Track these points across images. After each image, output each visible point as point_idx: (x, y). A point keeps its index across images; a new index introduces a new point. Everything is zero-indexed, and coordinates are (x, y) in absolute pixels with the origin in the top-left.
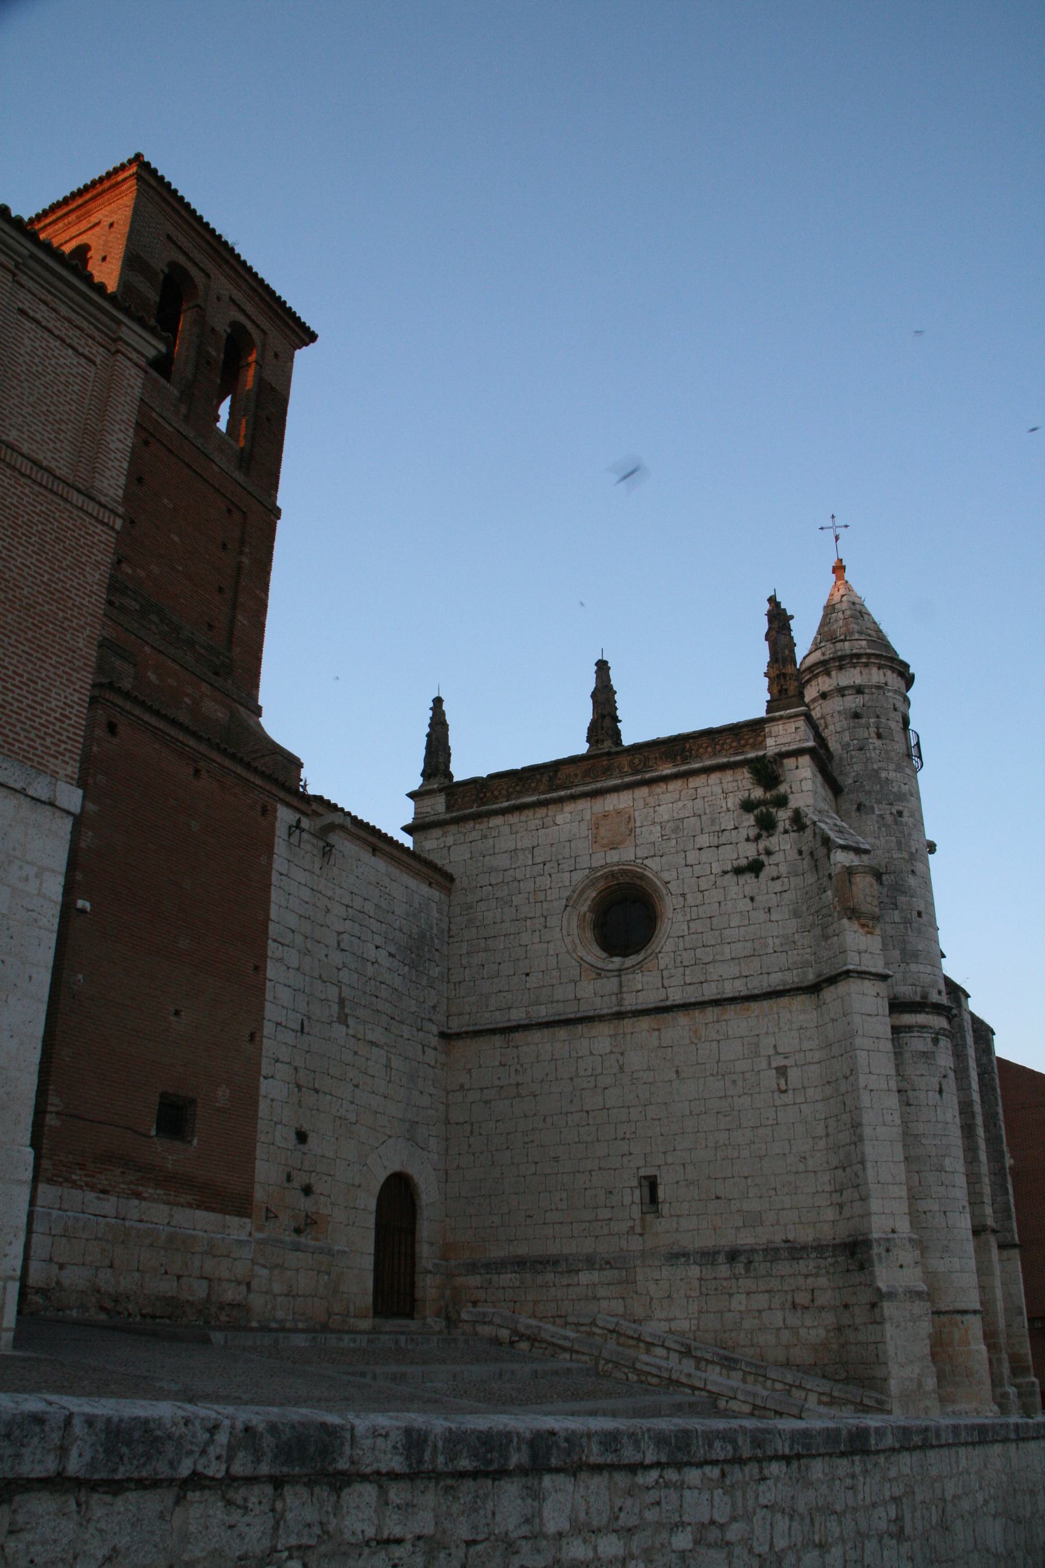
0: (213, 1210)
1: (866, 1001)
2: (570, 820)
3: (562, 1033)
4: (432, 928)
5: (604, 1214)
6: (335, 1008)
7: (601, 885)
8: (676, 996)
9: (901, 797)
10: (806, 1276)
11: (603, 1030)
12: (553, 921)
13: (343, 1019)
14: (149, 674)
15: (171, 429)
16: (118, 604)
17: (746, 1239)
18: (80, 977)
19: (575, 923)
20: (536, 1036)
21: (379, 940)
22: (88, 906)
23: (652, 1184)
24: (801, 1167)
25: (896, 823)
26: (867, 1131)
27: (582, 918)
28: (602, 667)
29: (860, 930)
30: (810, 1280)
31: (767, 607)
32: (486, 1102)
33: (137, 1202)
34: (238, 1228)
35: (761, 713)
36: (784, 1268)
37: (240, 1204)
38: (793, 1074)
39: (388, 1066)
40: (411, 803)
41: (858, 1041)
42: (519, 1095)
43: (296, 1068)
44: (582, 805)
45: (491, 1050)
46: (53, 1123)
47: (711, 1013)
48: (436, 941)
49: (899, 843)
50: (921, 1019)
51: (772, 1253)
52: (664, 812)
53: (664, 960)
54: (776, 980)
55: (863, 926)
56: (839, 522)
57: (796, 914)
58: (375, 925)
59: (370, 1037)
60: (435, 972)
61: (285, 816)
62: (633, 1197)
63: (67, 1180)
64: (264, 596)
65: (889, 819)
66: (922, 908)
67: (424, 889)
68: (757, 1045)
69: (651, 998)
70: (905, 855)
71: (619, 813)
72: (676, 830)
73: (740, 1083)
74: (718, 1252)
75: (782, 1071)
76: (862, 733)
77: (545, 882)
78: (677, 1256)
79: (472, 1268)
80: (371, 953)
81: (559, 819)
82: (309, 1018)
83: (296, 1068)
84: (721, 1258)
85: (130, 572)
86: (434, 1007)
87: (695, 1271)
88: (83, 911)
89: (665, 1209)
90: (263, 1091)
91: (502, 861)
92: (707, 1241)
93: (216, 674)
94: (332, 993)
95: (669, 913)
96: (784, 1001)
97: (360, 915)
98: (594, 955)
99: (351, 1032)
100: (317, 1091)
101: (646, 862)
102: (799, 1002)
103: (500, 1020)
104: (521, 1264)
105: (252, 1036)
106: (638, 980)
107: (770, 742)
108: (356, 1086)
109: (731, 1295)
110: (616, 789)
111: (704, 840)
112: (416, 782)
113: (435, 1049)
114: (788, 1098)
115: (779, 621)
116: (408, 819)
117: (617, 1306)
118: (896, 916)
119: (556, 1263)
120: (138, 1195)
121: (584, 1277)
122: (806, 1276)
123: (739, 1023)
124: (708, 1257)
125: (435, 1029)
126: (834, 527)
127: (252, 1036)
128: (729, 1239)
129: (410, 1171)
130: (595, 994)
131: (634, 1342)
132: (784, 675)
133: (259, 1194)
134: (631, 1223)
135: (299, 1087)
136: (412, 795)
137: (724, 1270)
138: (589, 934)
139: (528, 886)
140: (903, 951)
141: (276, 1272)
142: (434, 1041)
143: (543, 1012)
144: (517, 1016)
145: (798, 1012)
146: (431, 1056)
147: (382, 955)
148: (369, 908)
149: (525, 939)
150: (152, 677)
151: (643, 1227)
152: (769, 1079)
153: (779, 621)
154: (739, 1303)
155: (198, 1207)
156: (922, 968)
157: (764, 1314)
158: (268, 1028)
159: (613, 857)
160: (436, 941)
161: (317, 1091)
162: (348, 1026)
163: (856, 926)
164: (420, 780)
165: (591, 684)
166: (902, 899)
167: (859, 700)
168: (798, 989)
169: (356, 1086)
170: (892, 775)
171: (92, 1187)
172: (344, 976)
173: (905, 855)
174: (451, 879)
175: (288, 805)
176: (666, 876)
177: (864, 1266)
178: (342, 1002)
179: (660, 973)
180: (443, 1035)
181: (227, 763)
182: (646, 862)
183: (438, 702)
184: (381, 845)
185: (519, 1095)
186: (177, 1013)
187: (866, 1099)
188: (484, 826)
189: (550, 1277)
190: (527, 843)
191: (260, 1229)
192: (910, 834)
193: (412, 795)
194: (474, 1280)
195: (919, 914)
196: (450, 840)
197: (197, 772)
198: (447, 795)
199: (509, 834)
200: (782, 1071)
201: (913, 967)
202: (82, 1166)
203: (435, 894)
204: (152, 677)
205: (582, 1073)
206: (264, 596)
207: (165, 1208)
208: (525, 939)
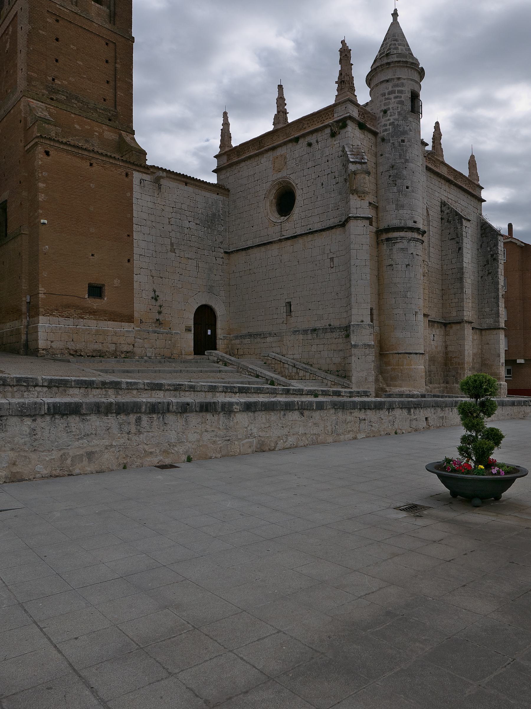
0: (116, 321)
3: (263, 249)
4: (219, 211)
5: (275, 316)
6: (169, 247)
7: (277, 187)
9: (404, 133)
10: (335, 338)
11: (275, 246)
13: (173, 251)
14: (75, 126)
15: (68, 11)
16: (55, 99)
17: (318, 325)
18: (47, 247)
19: (268, 204)
20: (256, 250)
21: (190, 219)
22: (46, 221)
23: (289, 304)
24: (337, 297)
25: (400, 145)
26: (353, 282)
29: (358, 199)
30: (337, 340)
31: (341, 46)
32: (241, 277)
33: (82, 320)
34: (127, 327)
36: (328, 335)
37: (130, 319)
39: (197, 266)
41: (352, 246)
42: (250, 274)
43: (151, 270)
44: (270, 154)
45: (241, 257)
46: (43, 297)
47: (310, 237)
48: (221, 216)
49: (400, 156)
50: (402, 234)
51: (325, 330)
55: (359, 197)
57: (340, 194)
58: (188, 213)
59: (187, 256)
61: (137, 176)
62: (283, 310)
63: (51, 315)
64: (130, 81)
65: (397, 144)
66: (409, 184)
67: (215, 196)
68: (324, 249)
70: (403, 161)
72: (300, 161)
73: (318, 265)
74: (308, 330)
78: (296, 331)
79: (237, 337)
80: (186, 224)
82: (156, 251)
83: (151, 270)
84: (309, 332)
85: (60, 83)
86: (221, 242)
87: (301, 337)
88: (44, 224)
89: (293, 314)
90: (135, 279)
92: (305, 326)
93: (110, 120)
94: (167, 241)
96: (334, 230)
97: (180, 210)
99: (177, 255)
100: (162, 278)
101: (291, 176)
102: (339, 231)
104: (250, 335)
105: (129, 261)
106: (287, 226)
107: (335, 115)
108: (182, 275)
109: (312, 345)
110: (280, 146)
111: (310, 164)
112: (217, 151)
113: (222, 258)
114: (333, 270)
116: (215, 167)
117: (278, 350)
118: (395, 189)
119: (260, 335)
120: (82, 318)
121: (269, 339)
122: (335, 338)
123: (320, 240)
124: (305, 332)
125: (222, 251)
127: (129, 261)
128: (312, 325)
129: (210, 303)
131: (279, 362)
132: (344, 81)
133: (136, 315)
134: (283, 320)
135: (152, 276)
137: (310, 336)
138: (274, 208)
140: (397, 205)
141: (146, 340)
142: (222, 255)
143: (257, 242)
144: (250, 244)
146: (220, 261)
147: (192, 225)
148: (184, 206)
150: (77, 127)
151: (287, 321)
153: (345, 54)
154: (314, 348)
155: (109, 320)
156: (405, 212)
157: (322, 352)
158: (136, 257)
159: (280, 175)
160: (221, 216)
161: (162, 278)
162: (175, 253)
163: (356, 197)
165: (276, 96)
168: (338, 225)
169: (182, 275)
170: (401, 122)
171: (62, 316)
172: (173, 234)
173: (403, 161)
174: (228, 190)
175: (138, 171)
177: (348, 336)
178: (172, 244)
180: (226, 252)
181: (104, 159)
182: (291, 176)
184: (188, 181)
185: (250, 274)
186: (93, 255)
188: (238, 167)
189: (259, 340)
191: (137, 327)
192: (407, 150)
194: (238, 341)
195: (407, 188)
196: (228, 174)
197: (91, 165)
198: (227, 155)
199: (246, 170)
200: (332, 259)
201: (401, 212)
202: (57, 310)
203: (220, 197)
204: (77, 127)
205: (269, 263)
206: (130, 81)
207: (95, 321)
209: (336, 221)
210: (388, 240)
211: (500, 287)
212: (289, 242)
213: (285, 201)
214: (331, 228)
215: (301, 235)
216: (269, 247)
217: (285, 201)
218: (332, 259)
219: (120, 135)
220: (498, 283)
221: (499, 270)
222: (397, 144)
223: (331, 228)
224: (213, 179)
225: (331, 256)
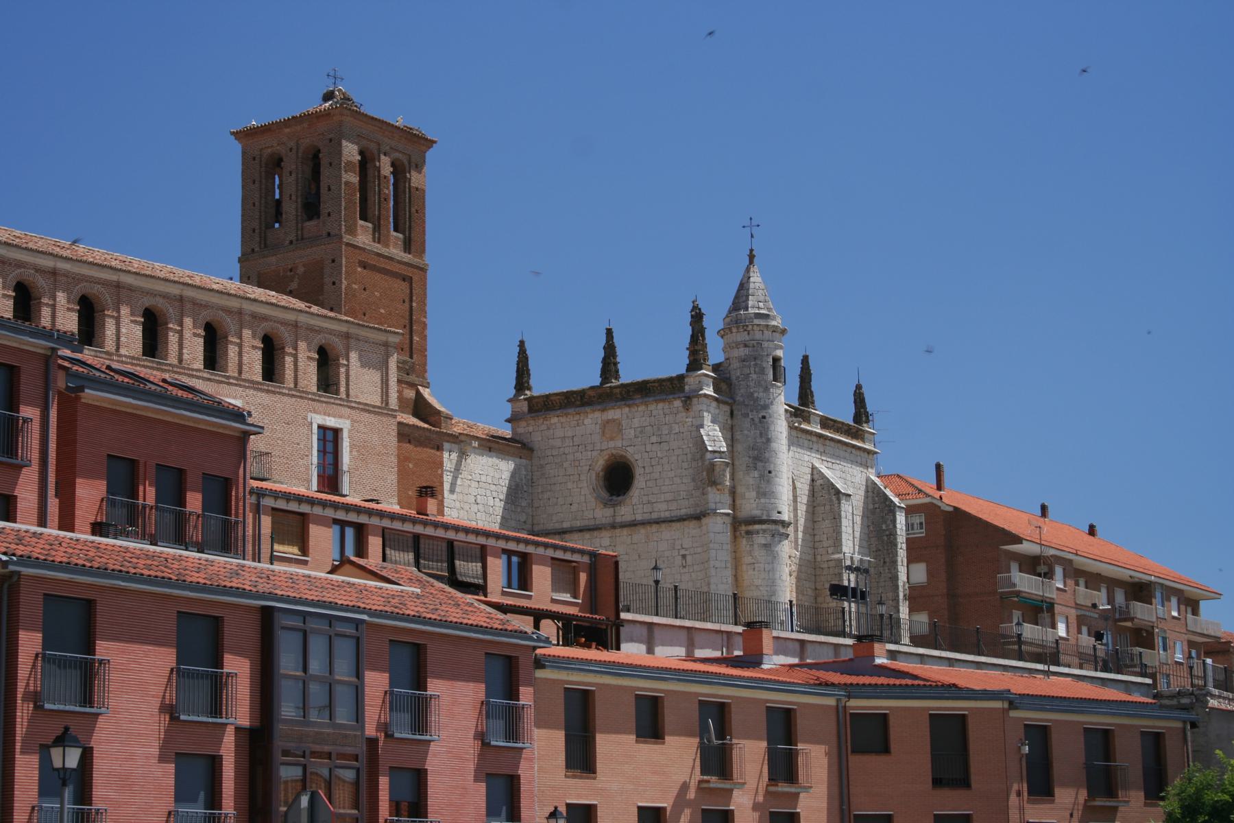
1: (717, 528)
2: (592, 420)
8: (639, 518)
12: (583, 477)
21: (495, 494)
27: (597, 475)
28: (609, 333)
35: (683, 370)
38: (689, 558)
40: (509, 405)
47: (654, 528)
52: (636, 422)
53: (635, 500)
54: (683, 512)
56: (754, 223)
57: (694, 480)
60: (524, 504)
65: (757, 420)
69: (628, 518)
71: (614, 420)
72: (641, 432)
75: (684, 556)
76: (746, 371)
77: (578, 455)
81: (586, 422)
91: (558, 443)
95: (637, 476)
96: (686, 523)
98: (604, 494)
103: (557, 526)
107: (687, 387)
111: (654, 439)
112: (512, 392)
114: (686, 570)
115: (697, 317)
118: (756, 474)
126: (751, 226)
130: (603, 515)
136: (508, 421)
138: (602, 483)
139: (570, 457)
140: (758, 493)
143: (578, 524)
144: (566, 525)
145: (691, 528)
149: (570, 485)
152: (679, 560)
153: (697, 317)
164: (514, 391)
165: (603, 340)
166: (760, 464)
167: (747, 351)
174: (532, 450)
176: (636, 457)
179: (633, 505)
183: (522, 344)
187: (713, 572)
190: (570, 434)
193: (508, 421)
201: (763, 500)
208: (570, 485)
209: (690, 511)
210: (748, 533)
211: (901, 584)
212: (625, 531)
213: (618, 478)
214: (681, 519)
215: (643, 523)
216: (596, 533)
217: (618, 478)
218: (684, 556)
219: (418, 393)
220: (896, 578)
221: (899, 559)
222: (757, 420)
223: (681, 519)
224: (506, 431)
225: (683, 552)
